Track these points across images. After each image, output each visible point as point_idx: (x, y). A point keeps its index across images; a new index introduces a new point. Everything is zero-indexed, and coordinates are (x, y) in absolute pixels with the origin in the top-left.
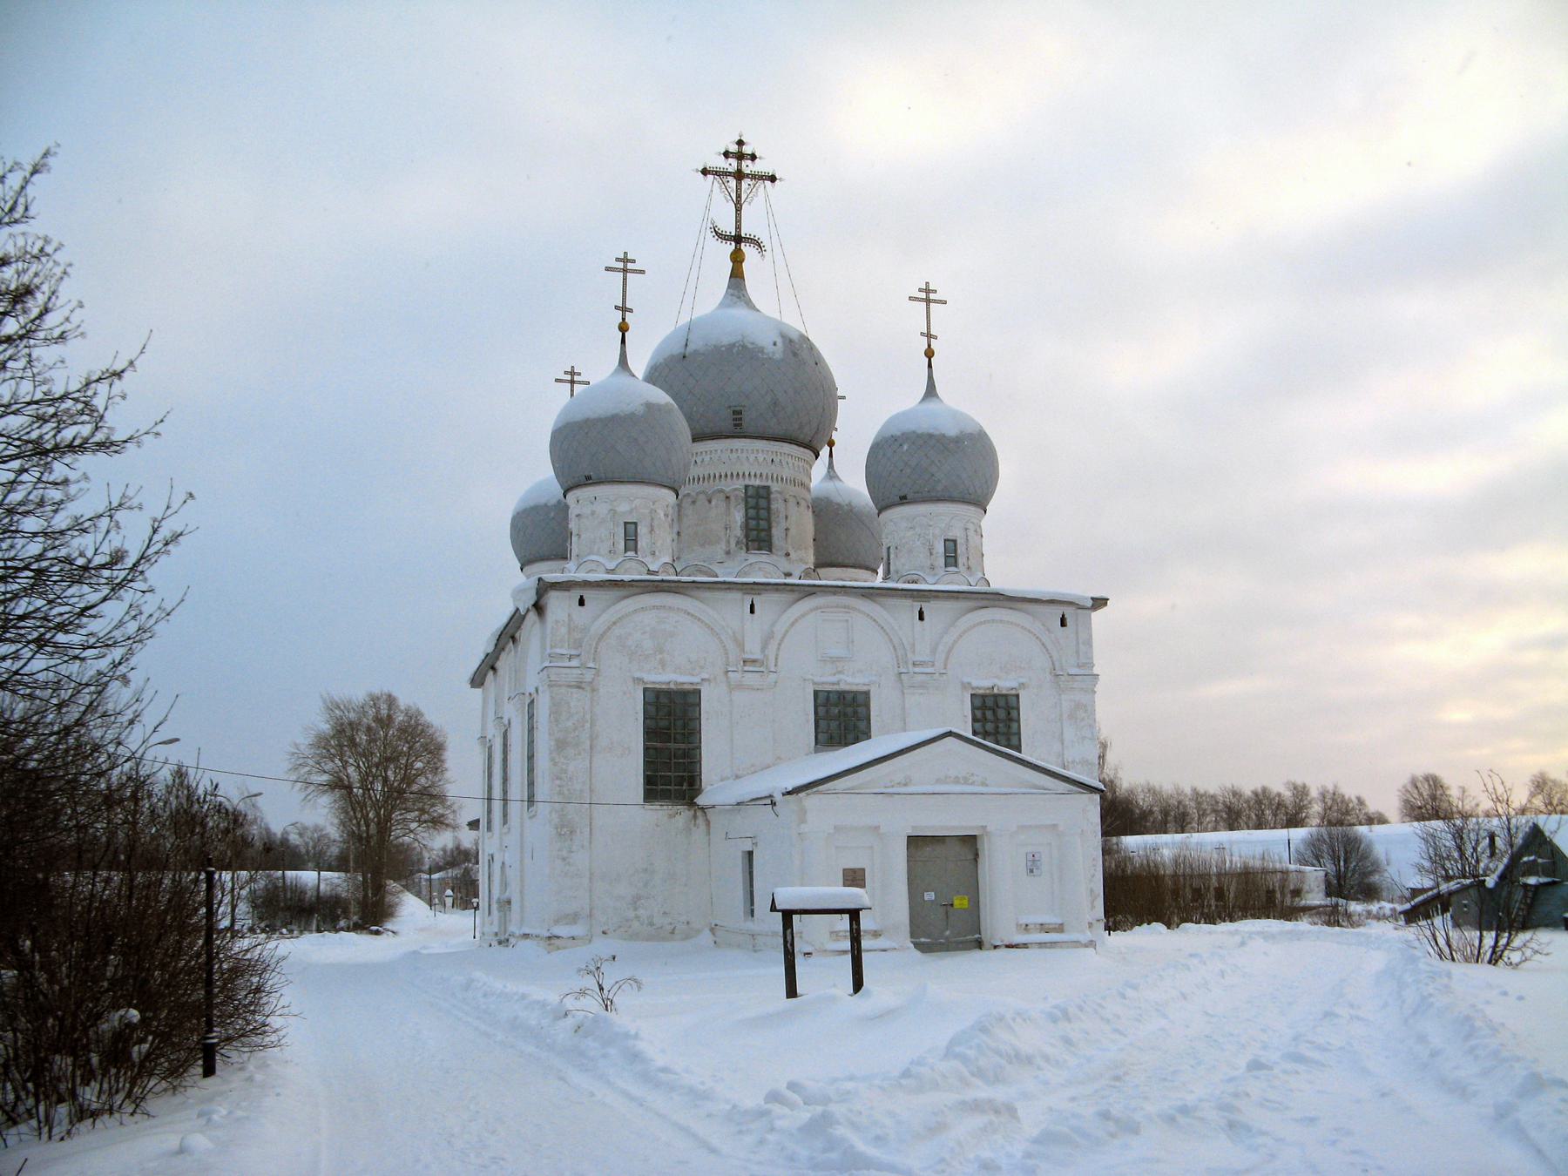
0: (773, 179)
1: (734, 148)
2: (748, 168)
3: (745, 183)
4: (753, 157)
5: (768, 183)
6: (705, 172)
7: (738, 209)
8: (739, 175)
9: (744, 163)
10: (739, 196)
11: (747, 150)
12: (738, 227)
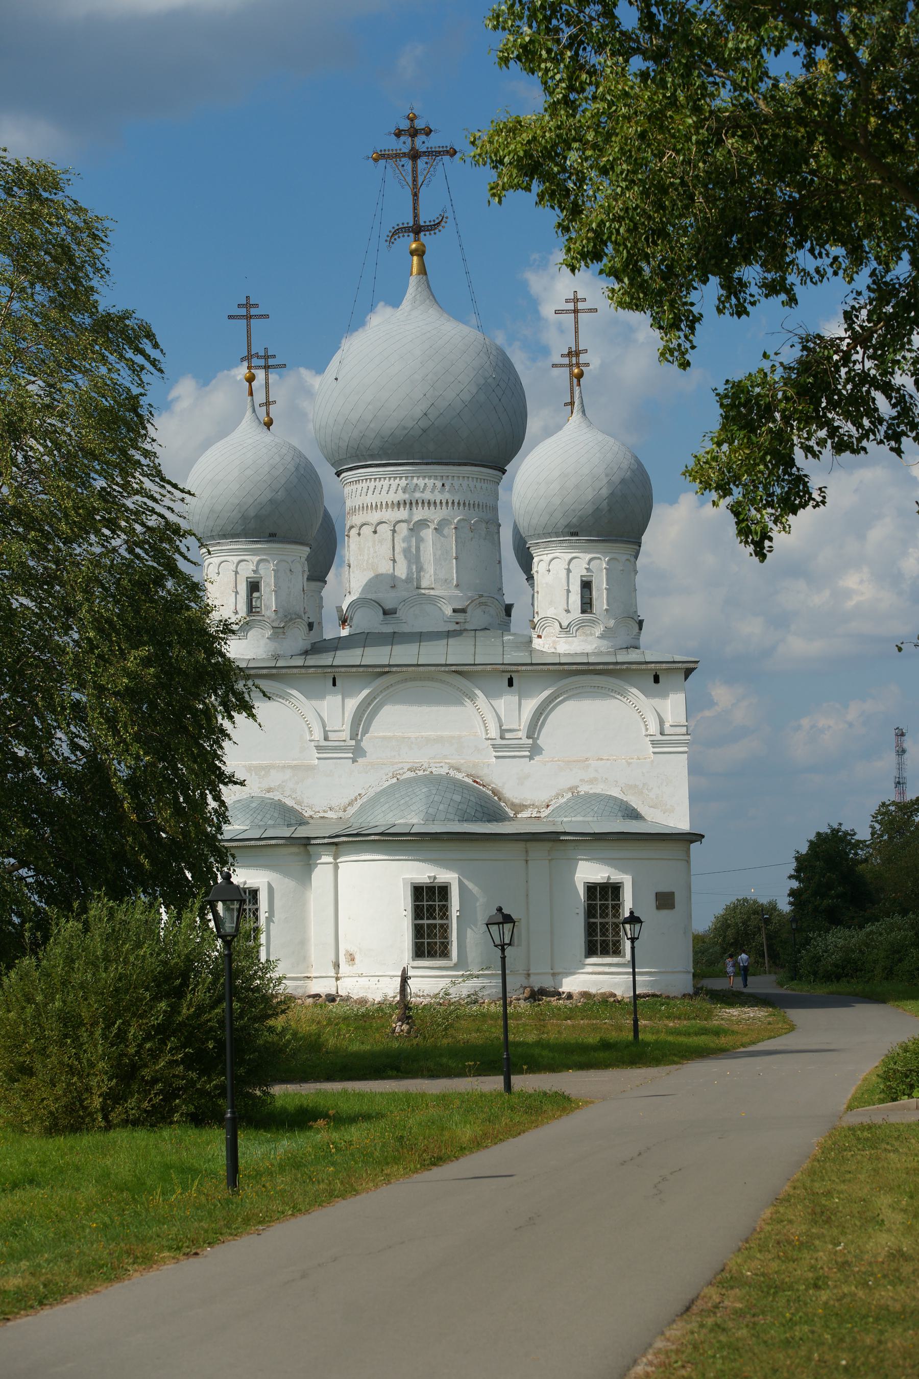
1: (405, 125)
2: (421, 143)
3: (421, 163)
4: (428, 132)
5: (446, 158)
7: (415, 195)
8: (415, 155)
9: (421, 138)
10: (415, 180)
11: (420, 124)
12: (416, 216)
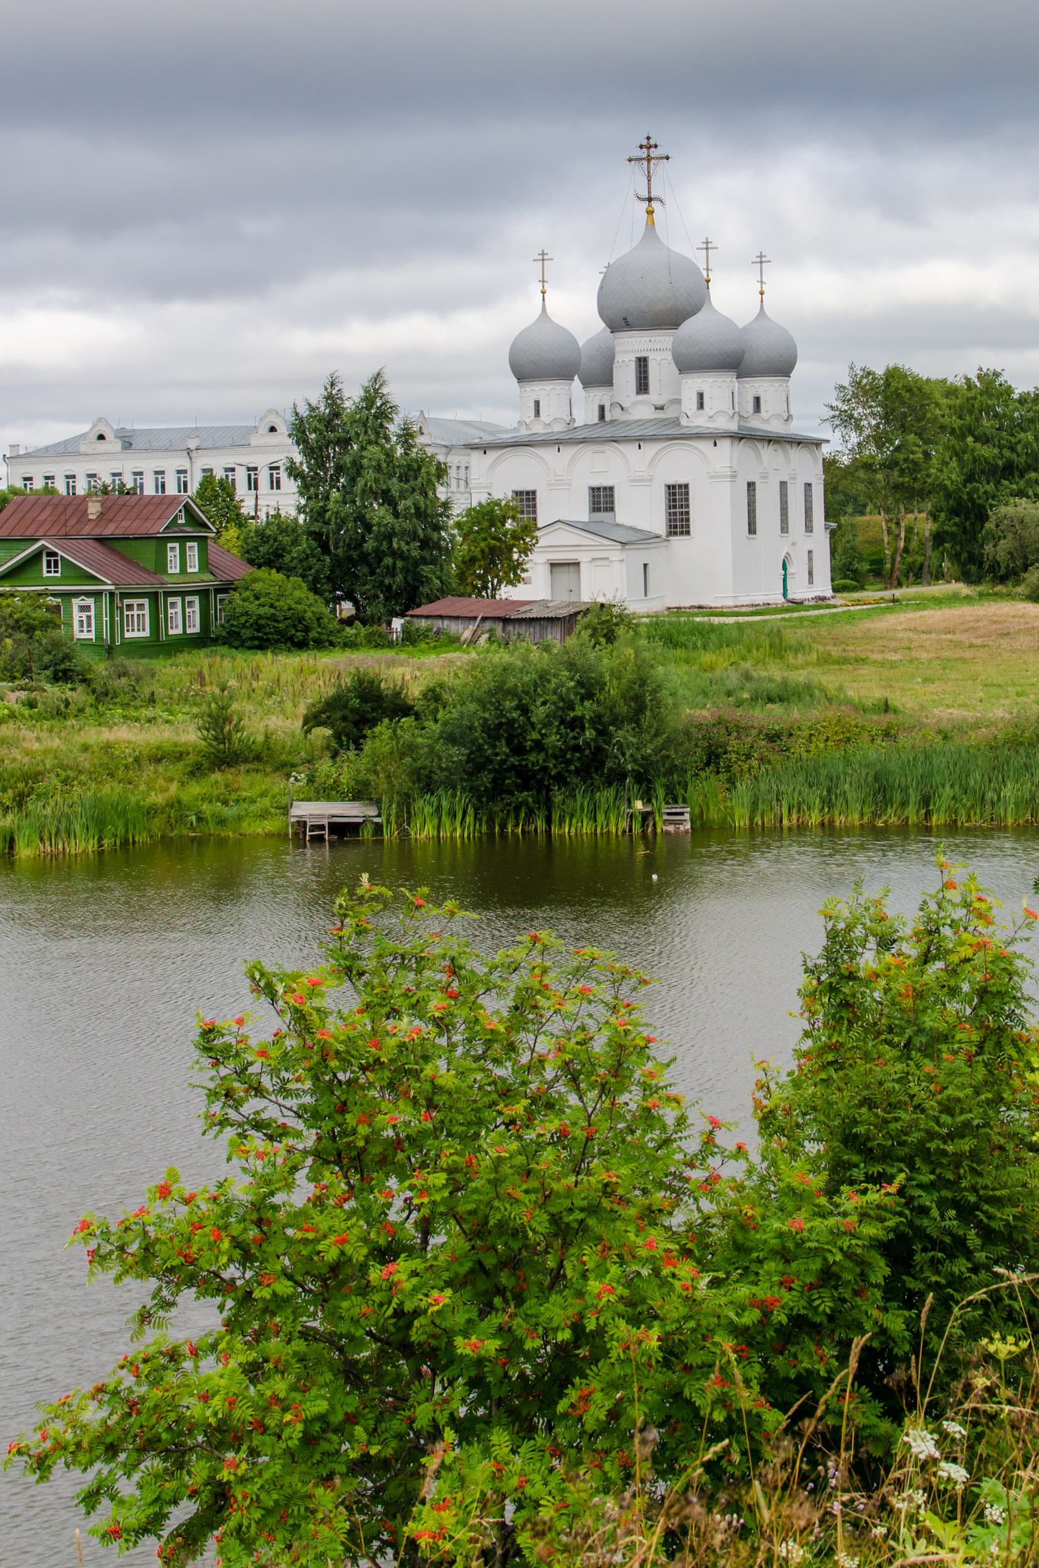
0: (667, 158)
1: (645, 142)
3: (653, 162)
4: (656, 146)
6: (630, 160)
9: (652, 149)
11: (652, 142)
